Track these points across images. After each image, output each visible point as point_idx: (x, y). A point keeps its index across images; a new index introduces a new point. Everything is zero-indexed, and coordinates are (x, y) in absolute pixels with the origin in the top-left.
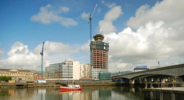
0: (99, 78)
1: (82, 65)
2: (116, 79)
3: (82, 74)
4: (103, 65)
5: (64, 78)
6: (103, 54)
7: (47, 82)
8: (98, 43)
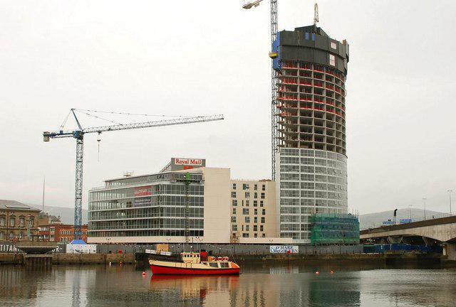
0: (310, 236)
1: (240, 187)
2: (378, 240)
5: (168, 233)
6: (325, 140)
7: (99, 250)
8: (307, 38)
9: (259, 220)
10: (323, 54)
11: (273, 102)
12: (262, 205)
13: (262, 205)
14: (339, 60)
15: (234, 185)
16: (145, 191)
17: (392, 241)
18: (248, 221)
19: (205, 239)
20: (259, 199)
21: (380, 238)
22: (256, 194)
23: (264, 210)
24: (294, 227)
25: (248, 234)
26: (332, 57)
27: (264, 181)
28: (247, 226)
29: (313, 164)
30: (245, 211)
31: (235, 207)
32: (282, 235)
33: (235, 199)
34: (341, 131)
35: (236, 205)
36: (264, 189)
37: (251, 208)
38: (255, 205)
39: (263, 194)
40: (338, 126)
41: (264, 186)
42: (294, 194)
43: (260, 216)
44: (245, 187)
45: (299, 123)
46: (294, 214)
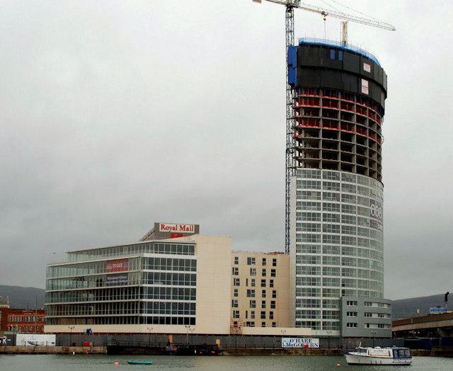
2: (424, 332)
3: (244, 302)
4: (354, 152)
5: (150, 321)
7: (58, 343)
9: (268, 305)
10: (353, 79)
11: (287, 150)
12: (272, 286)
13: (272, 286)
14: (377, 90)
15: (236, 258)
16: (120, 265)
17: (441, 332)
18: (254, 306)
19: (197, 329)
20: (268, 278)
21: (428, 330)
22: (264, 270)
23: (274, 292)
24: (313, 315)
25: (253, 323)
26: (365, 83)
27: (275, 253)
28: (253, 313)
29: (338, 190)
30: (250, 293)
31: (236, 287)
32: (298, 324)
33: (236, 277)
34: (375, 149)
35: (238, 284)
36: (274, 265)
37: (258, 289)
38: (263, 285)
39: (273, 271)
40: (372, 153)
41: (275, 260)
42: (314, 238)
43: (269, 299)
44: (251, 261)
45: (321, 148)
46: (314, 265)
